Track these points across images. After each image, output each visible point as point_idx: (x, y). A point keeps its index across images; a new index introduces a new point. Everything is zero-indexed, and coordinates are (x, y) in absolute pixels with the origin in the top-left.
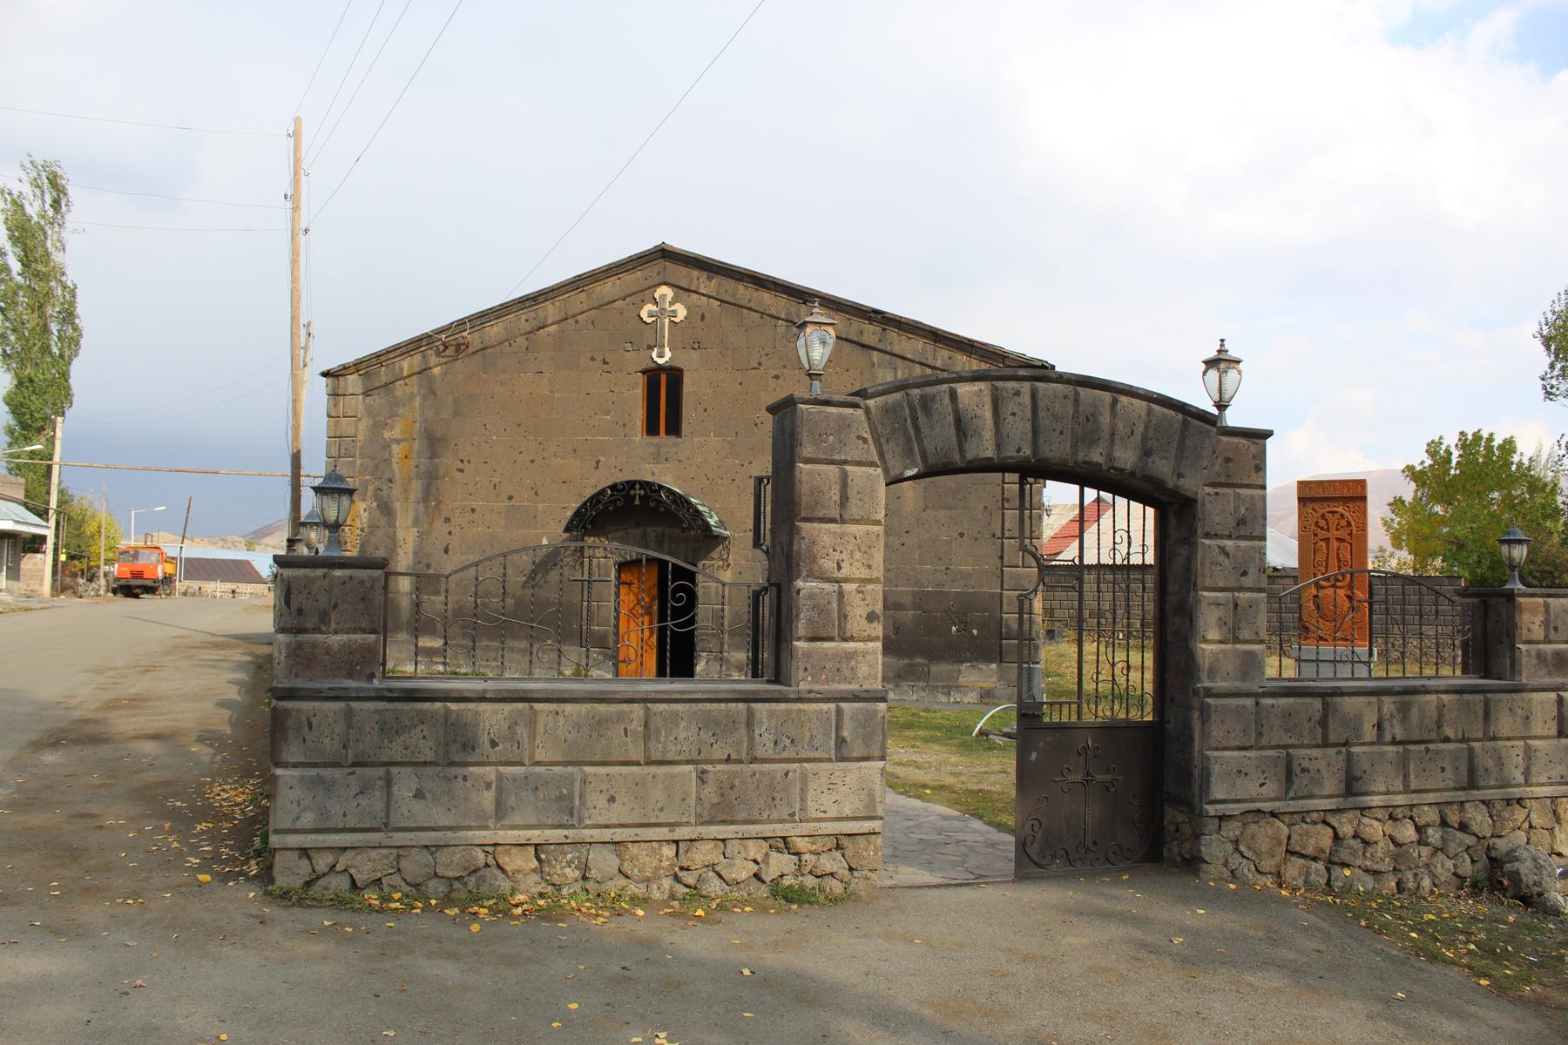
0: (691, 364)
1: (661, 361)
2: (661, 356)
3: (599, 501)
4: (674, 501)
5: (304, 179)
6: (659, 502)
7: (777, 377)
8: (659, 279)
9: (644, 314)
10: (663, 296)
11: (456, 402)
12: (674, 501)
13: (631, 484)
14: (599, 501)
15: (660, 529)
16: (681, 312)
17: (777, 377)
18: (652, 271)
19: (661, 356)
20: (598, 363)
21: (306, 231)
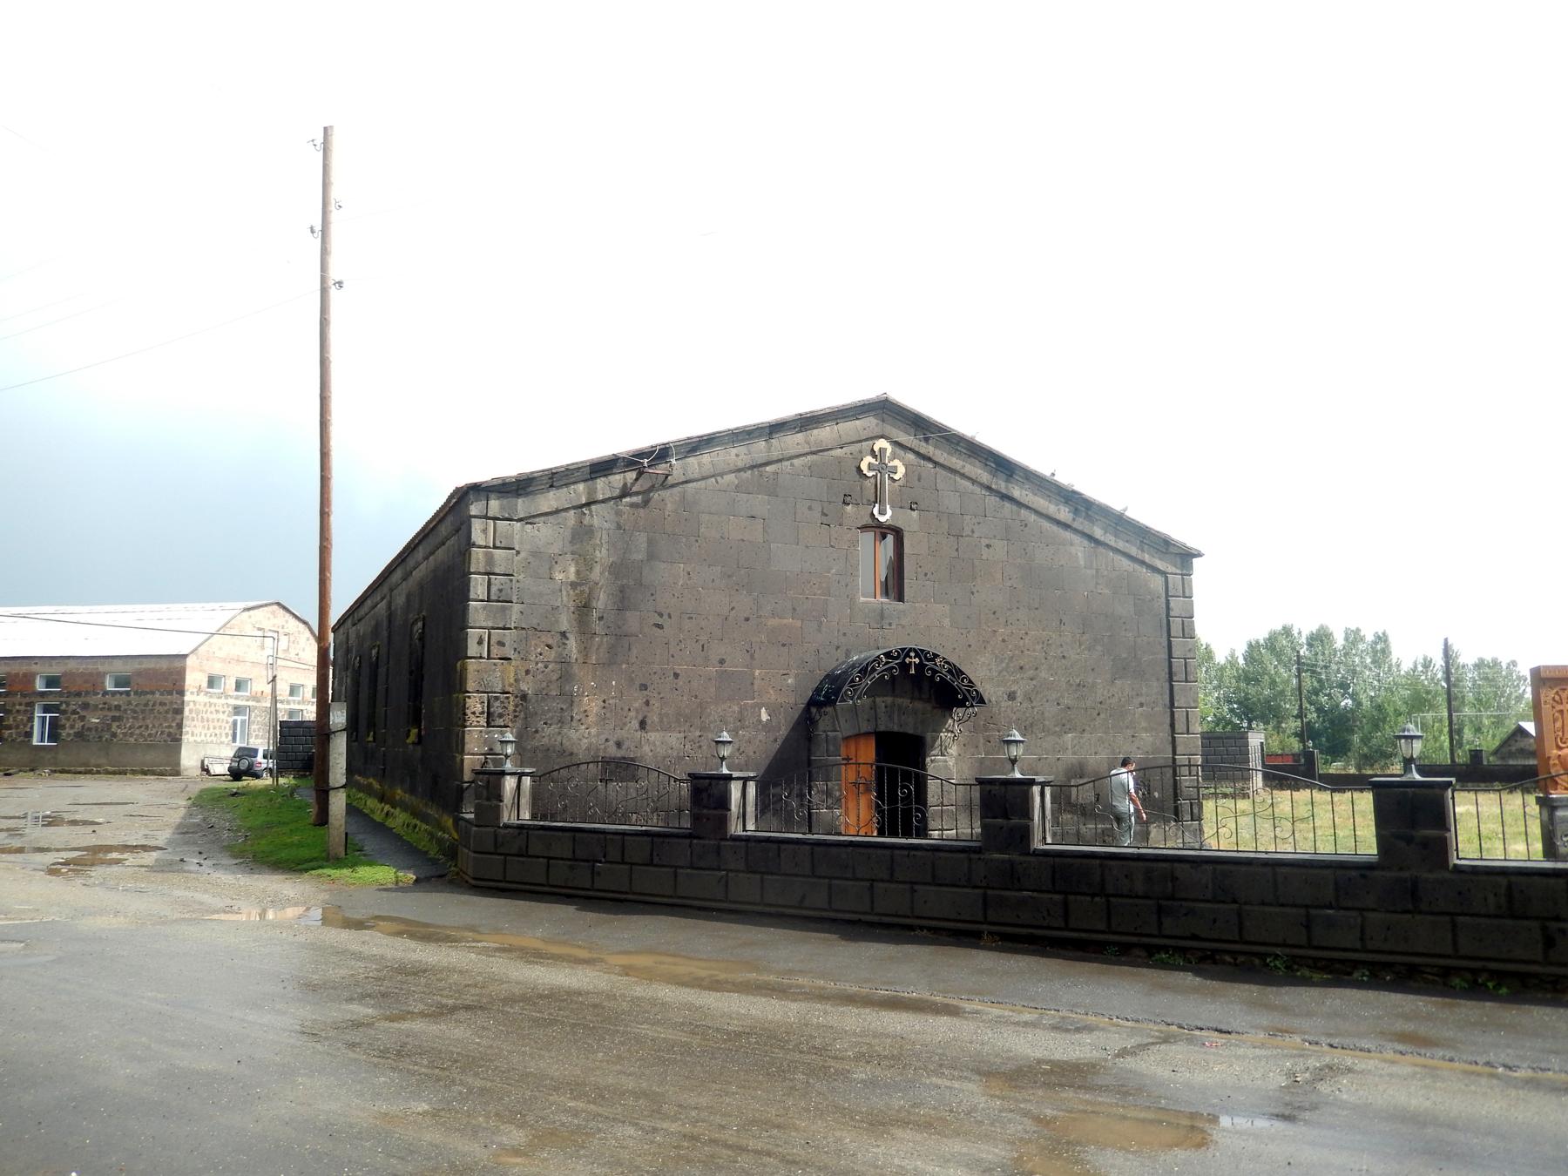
0: (910, 521)
1: (882, 519)
2: (882, 512)
3: (874, 670)
4: (950, 671)
5: (335, 216)
6: (935, 672)
7: (988, 546)
8: (877, 431)
9: (864, 466)
10: (882, 450)
11: (650, 542)
12: (950, 671)
13: (906, 652)
14: (874, 670)
15: (889, 700)
16: (901, 470)
17: (988, 546)
18: (869, 423)
19: (882, 512)
20: (817, 515)
21: (340, 284)
